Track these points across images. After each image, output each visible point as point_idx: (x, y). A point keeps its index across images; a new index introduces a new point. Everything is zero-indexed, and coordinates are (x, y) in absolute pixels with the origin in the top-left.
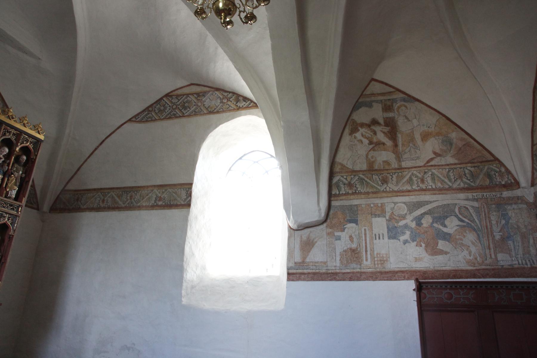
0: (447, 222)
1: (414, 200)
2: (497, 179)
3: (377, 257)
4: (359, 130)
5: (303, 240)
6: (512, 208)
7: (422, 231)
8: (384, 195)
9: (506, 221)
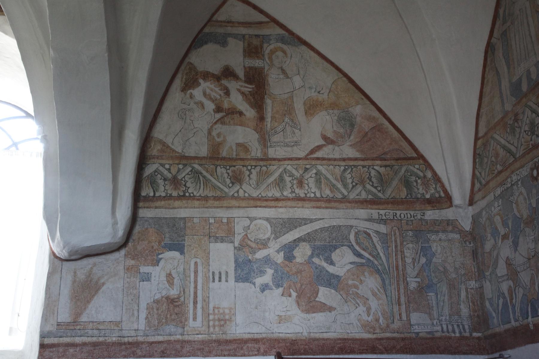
0: (335, 256)
1: (283, 216)
2: (418, 189)
3: (214, 314)
4: (199, 84)
5: (77, 280)
6: (438, 239)
7: (294, 270)
8: (234, 203)
9: (427, 260)
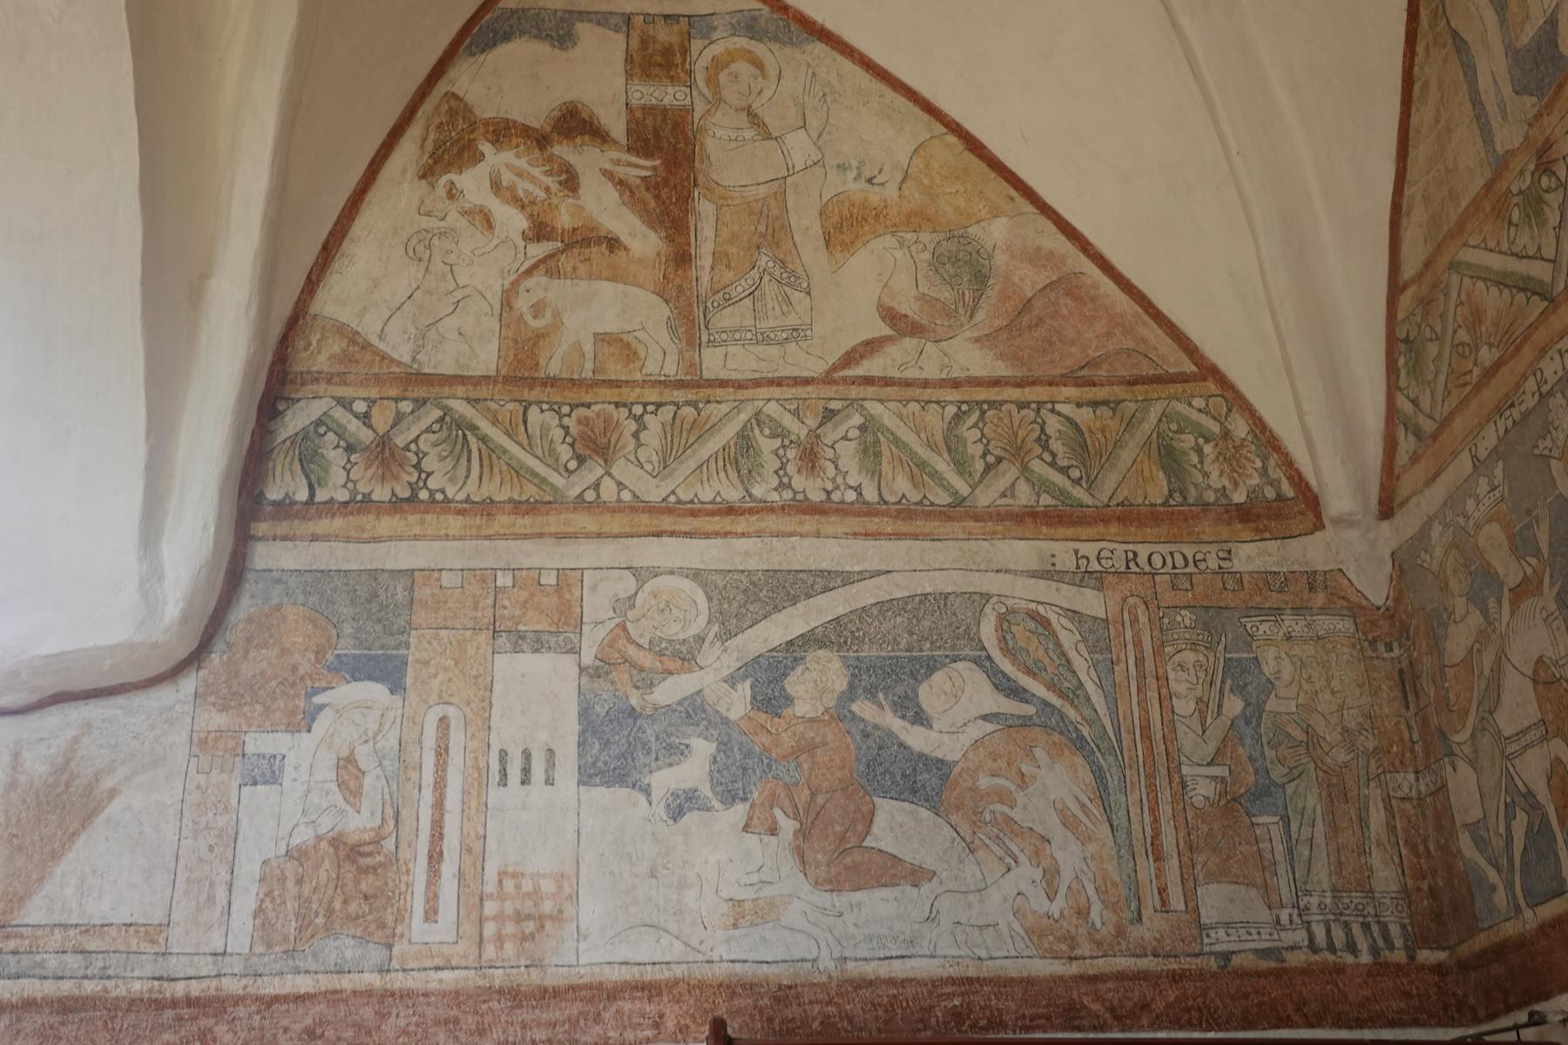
0: (930, 694)
1: (752, 564)
2: (1206, 475)
3: (501, 896)
4: (478, 158)
5: (23, 779)
6: (1281, 633)
7: (787, 741)
8: (584, 521)
9: (1248, 705)
